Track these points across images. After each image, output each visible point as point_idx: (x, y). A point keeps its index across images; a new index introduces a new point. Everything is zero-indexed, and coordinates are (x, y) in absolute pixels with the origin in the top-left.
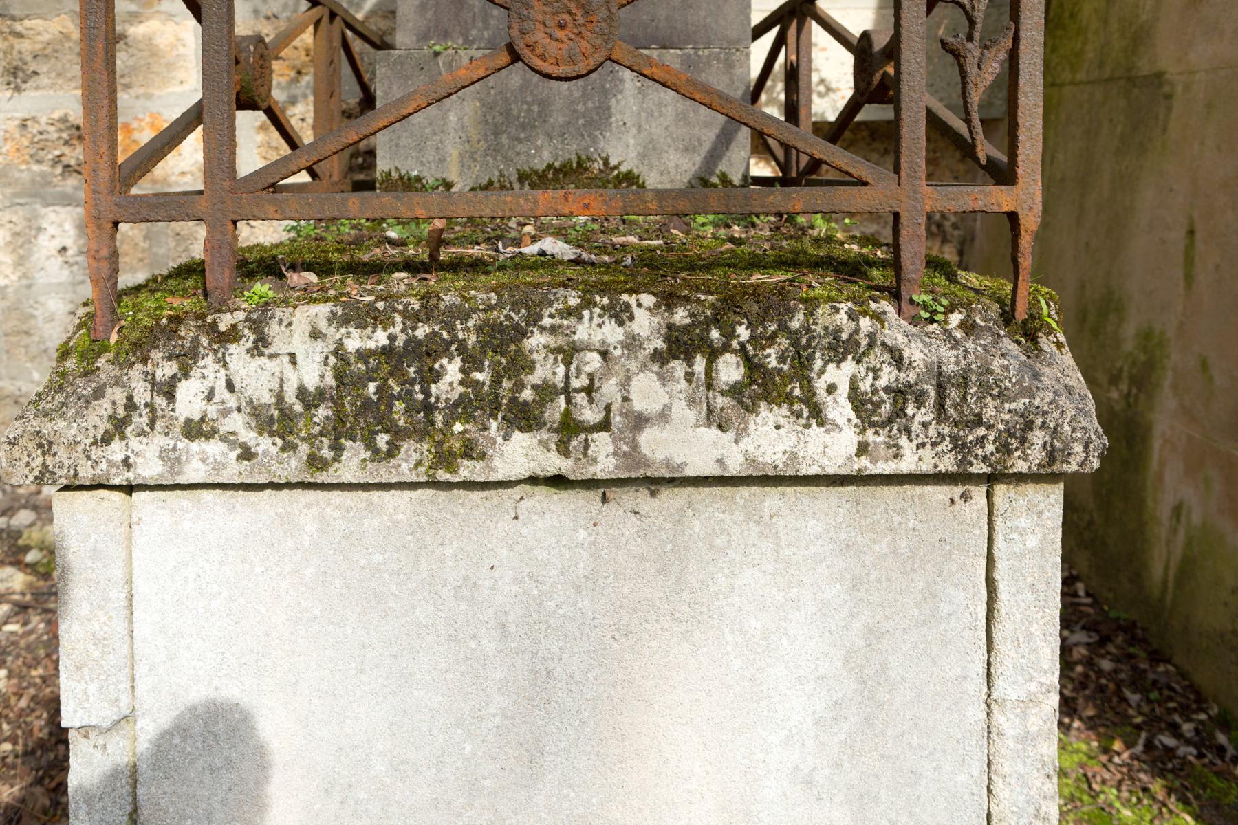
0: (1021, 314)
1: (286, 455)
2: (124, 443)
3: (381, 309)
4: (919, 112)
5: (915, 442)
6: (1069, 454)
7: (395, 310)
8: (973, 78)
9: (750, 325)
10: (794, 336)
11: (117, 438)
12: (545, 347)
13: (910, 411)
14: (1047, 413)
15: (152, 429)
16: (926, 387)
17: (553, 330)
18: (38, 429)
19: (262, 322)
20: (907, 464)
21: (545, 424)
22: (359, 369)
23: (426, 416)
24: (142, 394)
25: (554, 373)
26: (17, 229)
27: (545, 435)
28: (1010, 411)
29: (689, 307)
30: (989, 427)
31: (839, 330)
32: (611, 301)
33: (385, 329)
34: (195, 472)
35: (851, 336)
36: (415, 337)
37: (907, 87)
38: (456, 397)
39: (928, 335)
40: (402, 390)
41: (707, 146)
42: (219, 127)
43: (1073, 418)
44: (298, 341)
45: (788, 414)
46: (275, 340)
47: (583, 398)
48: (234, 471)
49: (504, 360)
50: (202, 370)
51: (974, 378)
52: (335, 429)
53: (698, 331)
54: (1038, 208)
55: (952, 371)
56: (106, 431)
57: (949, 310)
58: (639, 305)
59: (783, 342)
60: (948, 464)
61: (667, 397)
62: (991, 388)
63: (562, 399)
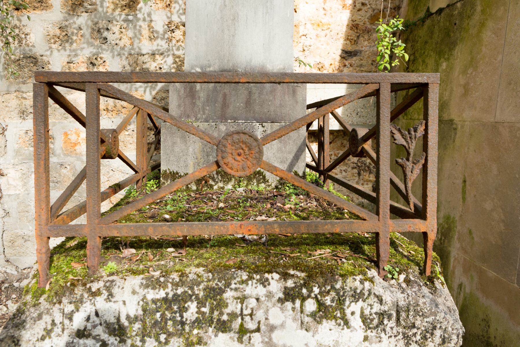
0: (428, 273)
1: (121, 344)
2: (51, 340)
3: (162, 281)
4: (387, 191)
5: (388, 335)
6: (451, 340)
7: (168, 282)
8: (409, 177)
9: (319, 287)
10: (337, 292)
11: (47, 338)
12: (232, 297)
13: (386, 322)
14: (442, 322)
15: (63, 333)
16: (392, 312)
17: (236, 289)
18: (13, 334)
19: (111, 287)
21: (232, 330)
22: (153, 307)
23: (182, 326)
24: (58, 318)
25: (236, 308)
26: (24, 172)
27: (232, 334)
28: (427, 322)
29: (293, 279)
30: (418, 329)
31: (356, 289)
32: (261, 277)
33: (164, 290)
35: (361, 291)
36: (177, 293)
37: (382, 180)
38: (195, 319)
39: (392, 286)
40: (171, 316)
41: (289, 161)
42: (93, 197)
43: (453, 324)
44: (126, 295)
45: (335, 324)
46: (116, 295)
47: (248, 319)
49: (215, 303)
50: (85, 308)
51: (412, 308)
52: (142, 332)
53: (297, 290)
54: (435, 230)
55: (403, 305)
56: (43, 335)
57: (399, 273)
58: (273, 279)
59: (333, 294)
61: (284, 317)
62: (419, 312)
63: (239, 320)
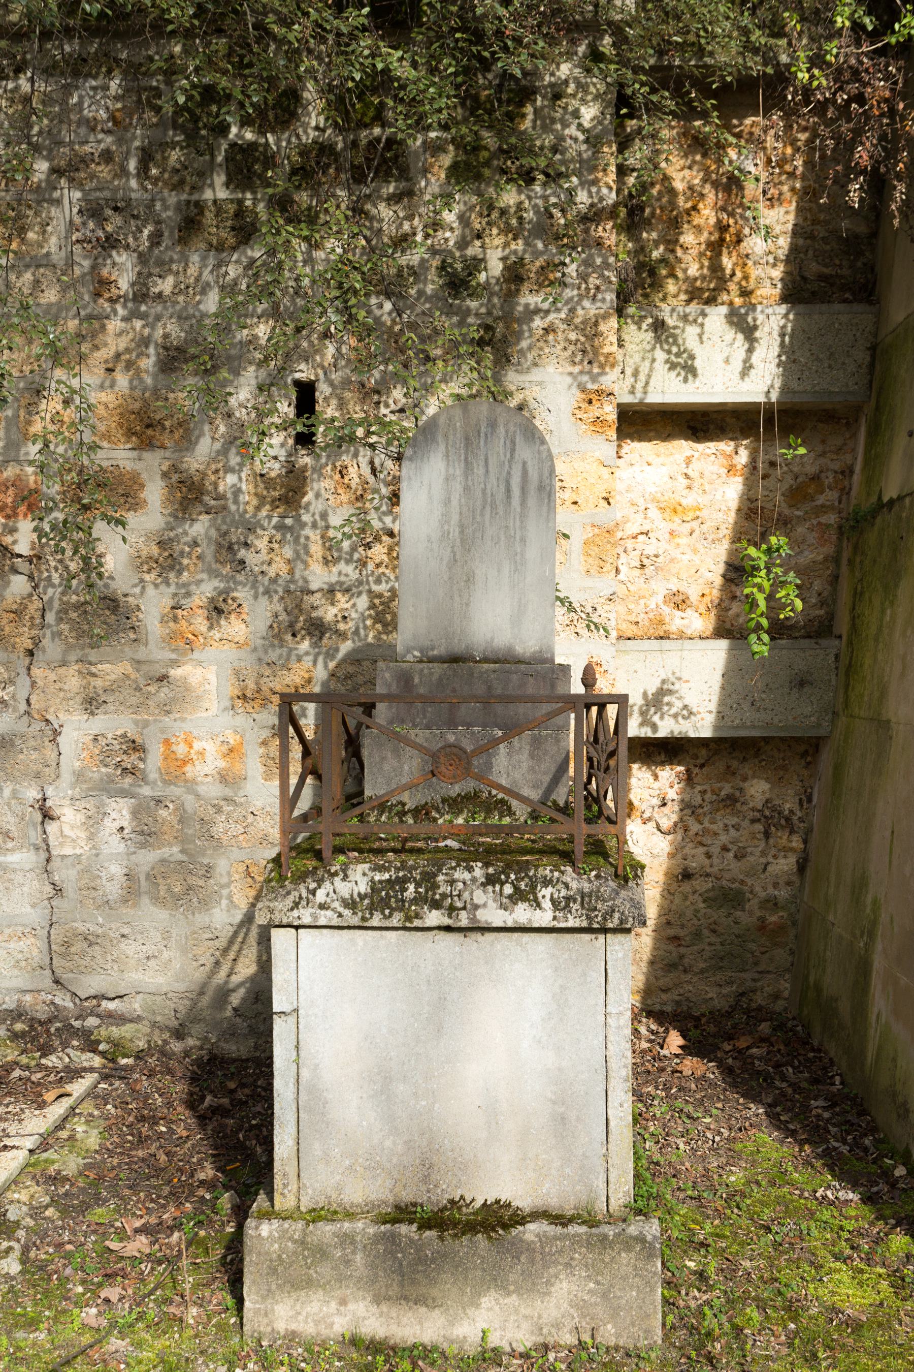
10: (530, 878)
17: (446, 874)
20: (571, 923)
24: (304, 894)
26: (90, 814)
34: (322, 921)
41: (545, 785)
44: (358, 876)
48: (336, 922)
57: (591, 870)
59: (527, 880)
60: (585, 924)
63: (449, 900)
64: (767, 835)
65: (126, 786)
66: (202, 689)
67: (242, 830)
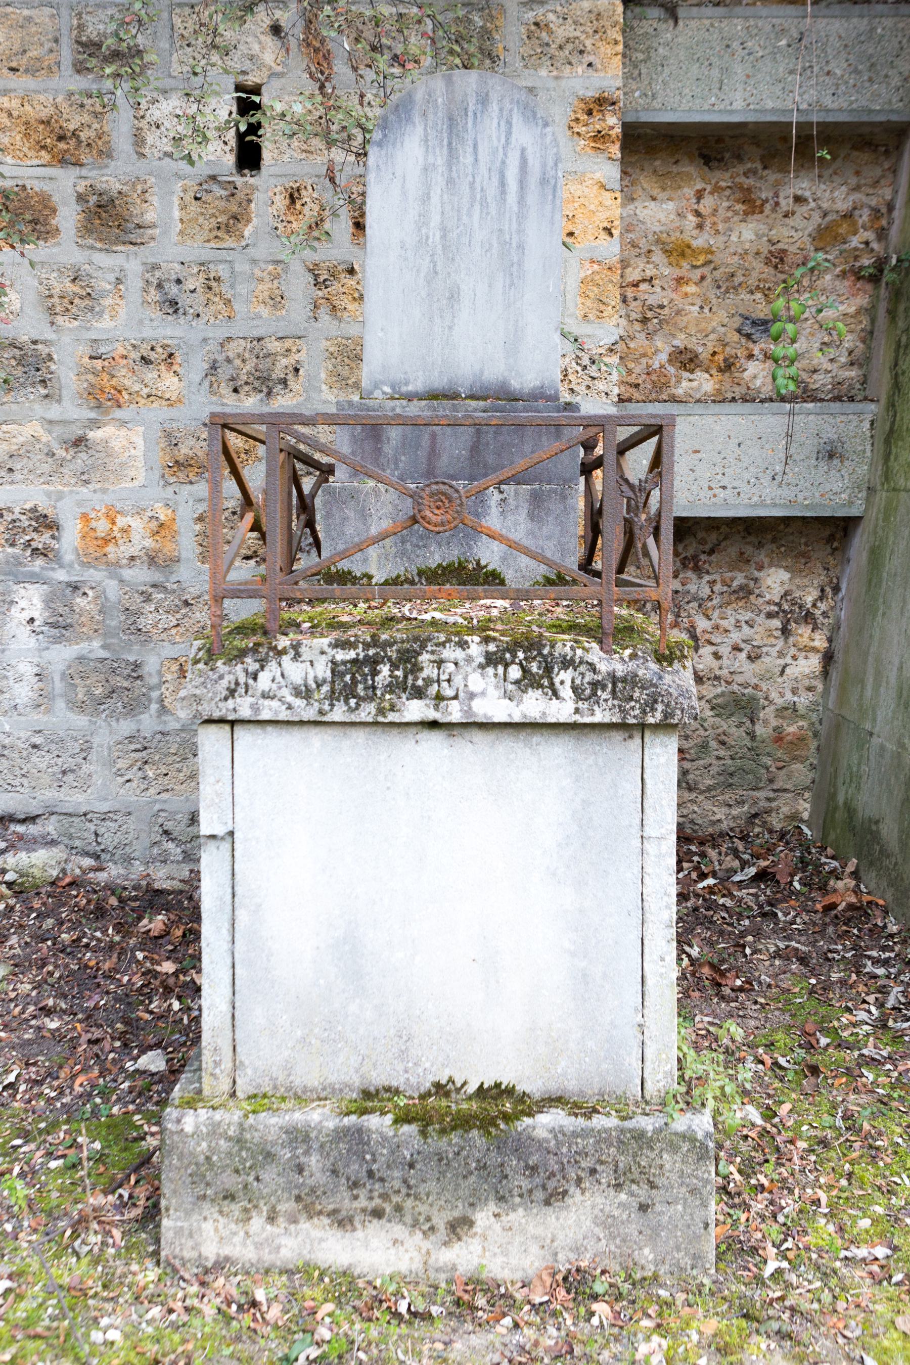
13: (599, 693)
17: (433, 652)
20: (600, 716)
24: (242, 679)
27: (428, 701)
30: (636, 701)
34: (265, 715)
48: (284, 715)
60: (616, 719)
63: (436, 685)
64: (785, 631)
65: (37, 569)
66: (127, 454)
67: (175, 622)
